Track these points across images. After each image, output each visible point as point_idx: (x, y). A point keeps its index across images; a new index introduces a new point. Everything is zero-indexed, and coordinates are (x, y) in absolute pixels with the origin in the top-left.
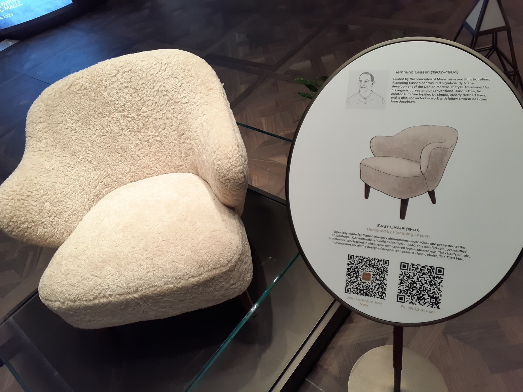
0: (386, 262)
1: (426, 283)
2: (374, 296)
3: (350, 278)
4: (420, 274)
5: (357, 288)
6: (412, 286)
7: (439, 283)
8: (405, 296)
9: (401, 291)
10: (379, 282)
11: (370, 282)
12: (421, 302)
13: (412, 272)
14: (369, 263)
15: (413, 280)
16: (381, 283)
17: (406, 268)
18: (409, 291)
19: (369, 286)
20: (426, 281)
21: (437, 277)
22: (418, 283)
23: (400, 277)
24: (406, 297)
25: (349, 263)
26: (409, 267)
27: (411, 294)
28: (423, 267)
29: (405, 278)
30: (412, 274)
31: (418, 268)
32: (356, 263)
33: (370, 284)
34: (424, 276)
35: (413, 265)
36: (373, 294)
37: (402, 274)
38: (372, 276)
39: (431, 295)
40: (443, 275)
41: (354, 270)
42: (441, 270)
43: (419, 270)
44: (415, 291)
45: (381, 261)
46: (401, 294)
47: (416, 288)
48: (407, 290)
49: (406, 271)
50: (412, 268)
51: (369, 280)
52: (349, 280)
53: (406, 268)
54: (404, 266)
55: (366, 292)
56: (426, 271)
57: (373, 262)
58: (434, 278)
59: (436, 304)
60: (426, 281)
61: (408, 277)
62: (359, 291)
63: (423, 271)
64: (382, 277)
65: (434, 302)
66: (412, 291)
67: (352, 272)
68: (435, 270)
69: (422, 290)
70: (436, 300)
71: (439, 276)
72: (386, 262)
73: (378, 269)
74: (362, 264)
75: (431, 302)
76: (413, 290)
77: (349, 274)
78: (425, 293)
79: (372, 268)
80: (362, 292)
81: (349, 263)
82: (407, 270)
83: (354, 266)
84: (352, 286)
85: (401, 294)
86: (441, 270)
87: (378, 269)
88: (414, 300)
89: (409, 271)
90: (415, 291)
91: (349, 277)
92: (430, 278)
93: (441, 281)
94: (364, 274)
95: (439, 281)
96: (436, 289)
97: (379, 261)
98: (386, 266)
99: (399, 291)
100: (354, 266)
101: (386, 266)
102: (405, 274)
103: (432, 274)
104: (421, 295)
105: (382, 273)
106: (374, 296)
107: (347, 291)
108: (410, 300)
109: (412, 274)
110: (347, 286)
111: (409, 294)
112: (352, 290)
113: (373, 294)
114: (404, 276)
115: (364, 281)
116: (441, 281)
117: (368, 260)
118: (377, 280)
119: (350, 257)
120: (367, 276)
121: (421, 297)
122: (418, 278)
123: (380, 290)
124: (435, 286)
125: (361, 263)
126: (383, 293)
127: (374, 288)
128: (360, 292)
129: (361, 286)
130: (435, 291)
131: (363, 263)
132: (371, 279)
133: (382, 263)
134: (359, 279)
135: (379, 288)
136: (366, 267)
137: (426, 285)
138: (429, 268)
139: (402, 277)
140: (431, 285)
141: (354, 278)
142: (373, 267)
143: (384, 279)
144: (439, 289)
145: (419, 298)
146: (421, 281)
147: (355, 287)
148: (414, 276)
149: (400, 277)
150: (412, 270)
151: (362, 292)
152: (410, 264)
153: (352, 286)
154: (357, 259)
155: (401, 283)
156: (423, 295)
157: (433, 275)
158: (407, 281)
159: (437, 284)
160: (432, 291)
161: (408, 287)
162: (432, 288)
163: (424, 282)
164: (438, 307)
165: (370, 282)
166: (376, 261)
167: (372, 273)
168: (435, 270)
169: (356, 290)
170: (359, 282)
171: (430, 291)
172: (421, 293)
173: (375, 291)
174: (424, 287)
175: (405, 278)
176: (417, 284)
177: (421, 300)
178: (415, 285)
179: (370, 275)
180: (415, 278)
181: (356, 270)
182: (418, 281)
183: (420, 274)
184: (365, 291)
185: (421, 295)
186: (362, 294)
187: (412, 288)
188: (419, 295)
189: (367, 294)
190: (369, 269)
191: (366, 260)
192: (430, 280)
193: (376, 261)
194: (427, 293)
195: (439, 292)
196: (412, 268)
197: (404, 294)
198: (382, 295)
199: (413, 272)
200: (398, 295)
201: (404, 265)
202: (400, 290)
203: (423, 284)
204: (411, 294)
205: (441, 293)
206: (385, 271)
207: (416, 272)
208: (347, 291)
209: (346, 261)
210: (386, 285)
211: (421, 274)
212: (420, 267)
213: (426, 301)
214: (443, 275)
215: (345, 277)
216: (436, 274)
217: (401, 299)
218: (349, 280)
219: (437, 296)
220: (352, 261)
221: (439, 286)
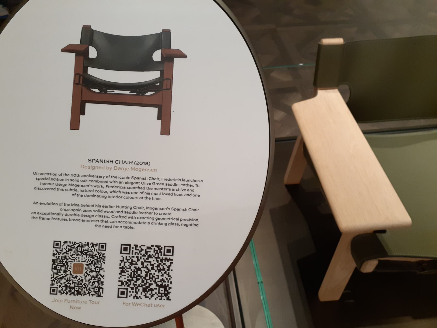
0: (103, 246)
1: (153, 269)
2: (89, 293)
3: (57, 274)
4: (145, 258)
5: (66, 286)
6: (135, 276)
7: (169, 267)
8: (127, 289)
9: (122, 283)
10: (94, 274)
11: (82, 275)
12: (148, 295)
13: (135, 256)
14: (81, 249)
15: (137, 266)
16: (97, 276)
17: (128, 252)
18: (132, 282)
19: (82, 280)
20: (153, 265)
21: (166, 259)
22: (143, 269)
23: (120, 265)
24: (129, 289)
25: (55, 252)
26: (132, 249)
27: (135, 285)
28: (148, 248)
29: (127, 264)
30: (135, 259)
31: (142, 250)
32: (64, 251)
33: (83, 278)
34: (150, 260)
35: (136, 246)
36: (87, 292)
37: (123, 260)
38: (85, 266)
39: (159, 284)
40: (172, 255)
41: (61, 262)
42: (170, 250)
43: (143, 252)
44: (140, 281)
45: (96, 245)
46: (123, 287)
47: (141, 277)
48: (130, 281)
49: (128, 255)
50: (135, 251)
51: (82, 273)
52: (55, 276)
53: (128, 252)
54: (125, 249)
55: (76, 289)
56: (152, 252)
57: (86, 247)
58: (162, 260)
59: (166, 295)
60: (153, 265)
61: (131, 263)
62: (68, 289)
63: (149, 253)
64: (97, 267)
65: (163, 292)
66: (136, 282)
67: (59, 264)
68: (162, 251)
69: (148, 278)
70: (166, 290)
71: (168, 257)
72: (103, 246)
73: (92, 256)
74: (72, 253)
75: (159, 293)
76: (137, 280)
77: (55, 268)
78: (152, 282)
79: (85, 256)
80: (73, 291)
81: (55, 252)
82: (129, 254)
83: (61, 255)
84: (59, 284)
85: (123, 287)
86: (170, 250)
87: (92, 256)
88: (139, 293)
89: (131, 255)
90: (140, 281)
91: (55, 271)
92: (158, 261)
93: (171, 263)
94: (74, 264)
95: (168, 263)
96: (165, 275)
97: (93, 245)
98: (103, 252)
99: (120, 283)
100: (61, 255)
101: (103, 252)
102: (126, 259)
103: (160, 256)
104: (147, 285)
105: (98, 262)
106: (89, 293)
107: (53, 291)
108: (134, 294)
109: (135, 259)
110: (52, 284)
111: (132, 286)
112: (59, 289)
113: (87, 292)
114: (125, 263)
115: (74, 275)
116: (171, 263)
117: (79, 246)
118: (92, 271)
119: (57, 244)
120: (78, 268)
121: (147, 287)
122: (142, 264)
123: (96, 284)
124: (163, 272)
125: (71, 250)
126: (100, 288)
127: (87, 283)
128: (70, 291)
129: (71, 282)
130: (164, 277)
131: (74, 250)
132: (84, 271)
133: (97, 248)
134: (68, 273)
135: (94, 282)
136: (78, 255)
137: (152, 272)
138: (156, 249)
139: (122, 264)
140: (159, 271)
141: (62, 272)
142: (86, 254)
143: (101, 269)
144: (168, 275)
145: (144, 290)
146: (146, 267)
147: (63, 285)
148: (138, 260)
149: (120, 265)
150: (136, 253)
151: (73, 291)
152: (132, 246)
153: (59, 284)
154: (65, 246)
155: (122, 272)
156: (150, 285)
157: (161, 257)
158: (130, 268)
159: (167, 269)
160: (161, 278)
161: (131, 276)
162: (160, 274)
163: (150, 267)
164: (168, 299)
165: (82, 275)
166: (90, 246)
167: (85, 263)
168: (162, 251)
169: (64, 288)
170: (68, 276)
171: (158, 278)
172: (147, 282)
173: (89, 286)
174: (150, 274)
175: (127, 264)
176: (141, 271)
177: (148, 292)
178: (139, 272)
179: (83, 265)
180: (139, 263)
181: (65, 261)
182: (143, 267)
183: (145, 258)
184: (77, 288)
185: (147, 285)
186: (73, 293)
187: (136, 278)
188: (144, 285)
189: (79, 293)
190: (81, 257)
191: (77, 245)
192: (157, 264)
193: (90, 246)
194: (155, 281)
195: (168, 278)
196: (135, 251)
197: (126, 287)
198: (99, 291)
199: (137, 255)
200: (119, 289)
201: (125, 248)
202: (121, 281)
203: (149, 271)
204: (135, 285)
205: (171, 280)
206: (102, 258)
207: (140, 256)
208: (53, 291)
209: (51, 250)
210: (103, 277)
211: (147, 257)
212: (144, 248)
213: (154, 292)
214: (172, 255)
215: (49, 273)
216: (164, 255)
217: (123, 293)
218: (55, 276)
219: (166, 284)
220: (58, 250)
221: (169, 270)
